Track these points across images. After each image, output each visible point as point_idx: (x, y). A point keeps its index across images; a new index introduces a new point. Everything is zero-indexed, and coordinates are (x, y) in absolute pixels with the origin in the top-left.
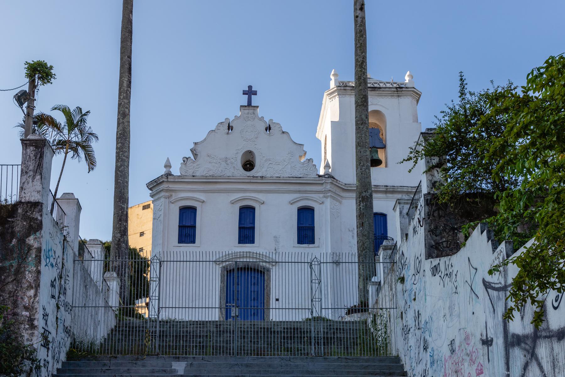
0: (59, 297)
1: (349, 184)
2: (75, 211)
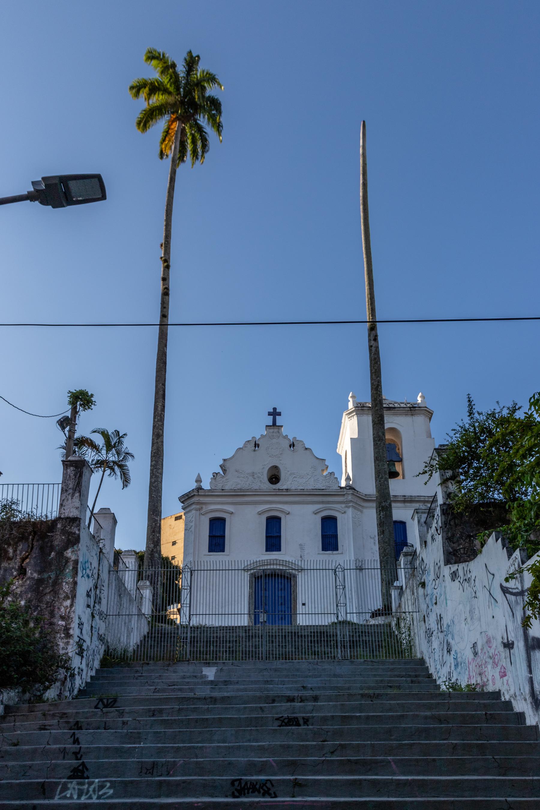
0: (94, 606)
1: (369, 495)
2: (111, 524)
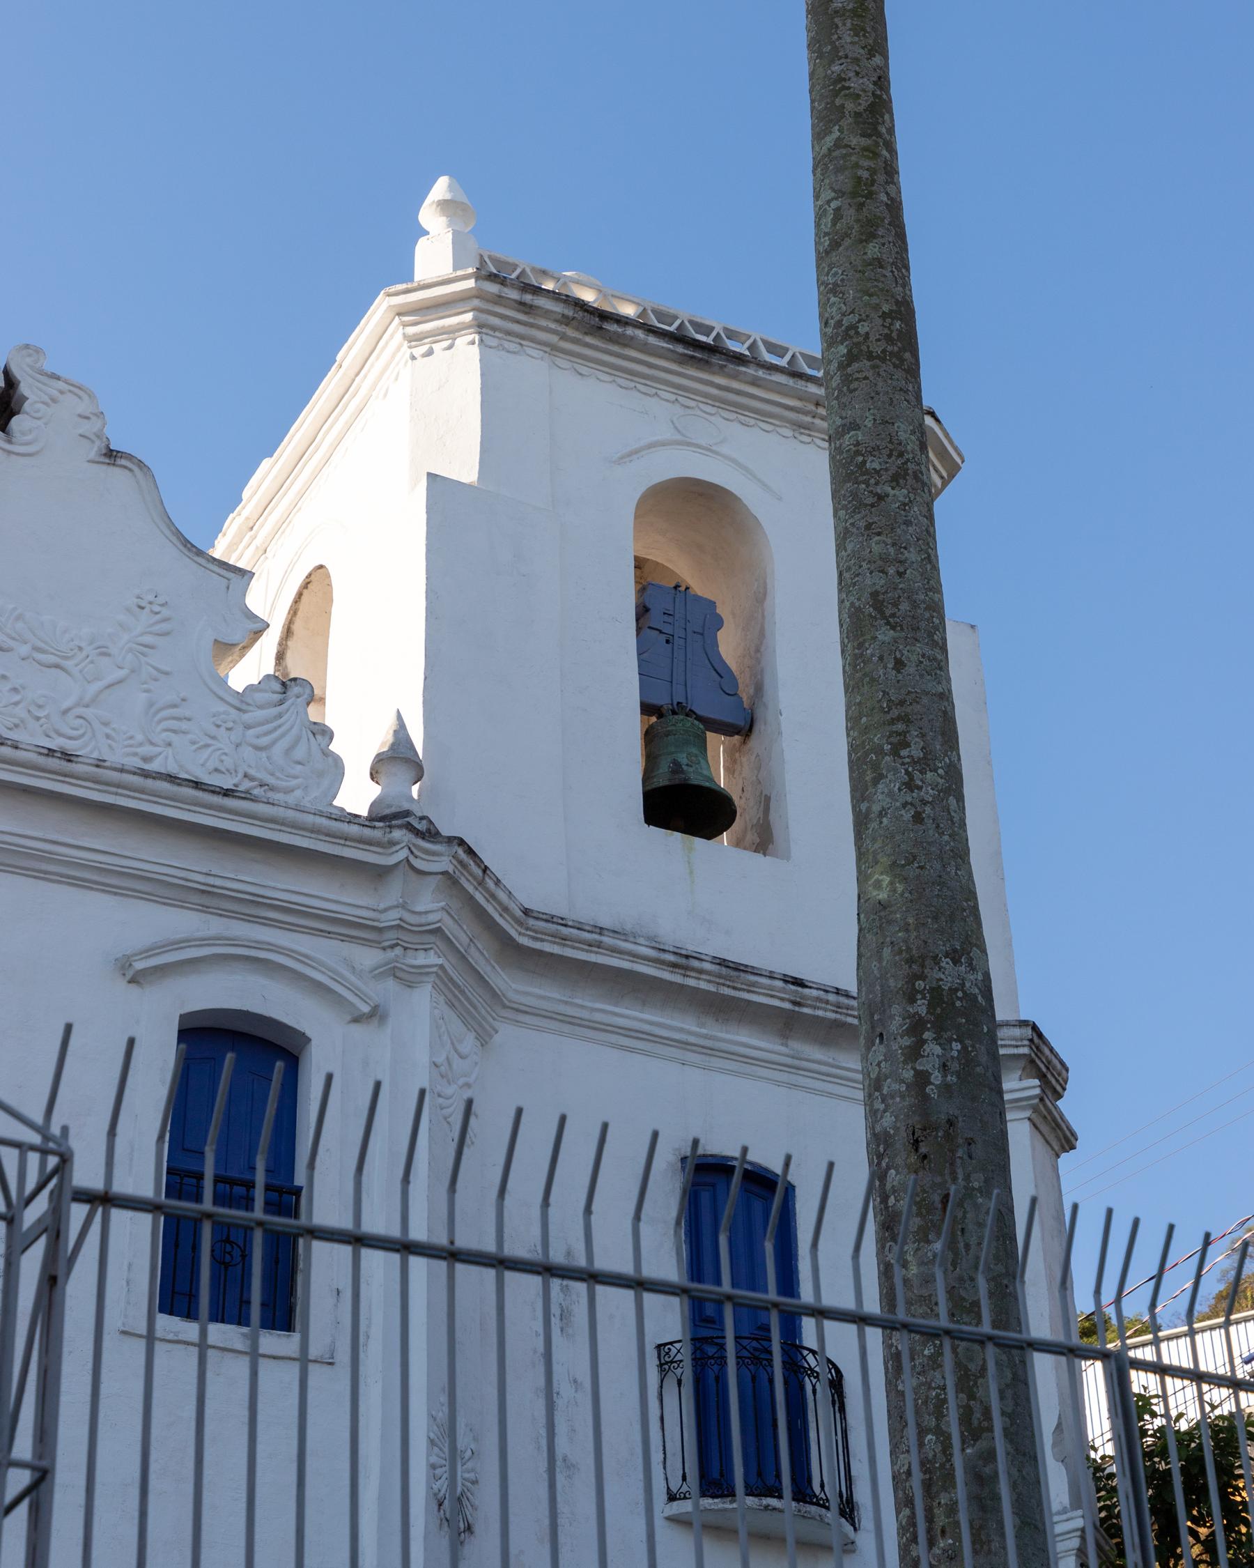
1: (550, 919)
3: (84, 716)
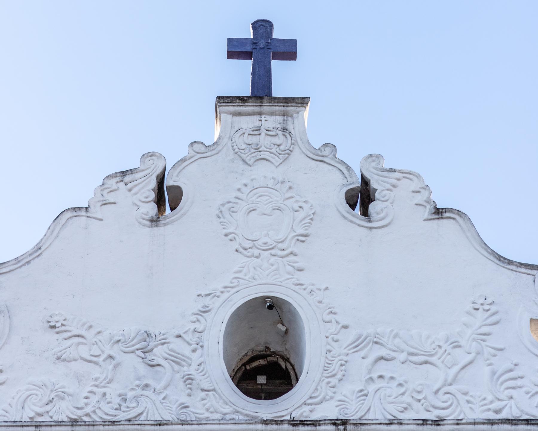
3: (450, 392)
